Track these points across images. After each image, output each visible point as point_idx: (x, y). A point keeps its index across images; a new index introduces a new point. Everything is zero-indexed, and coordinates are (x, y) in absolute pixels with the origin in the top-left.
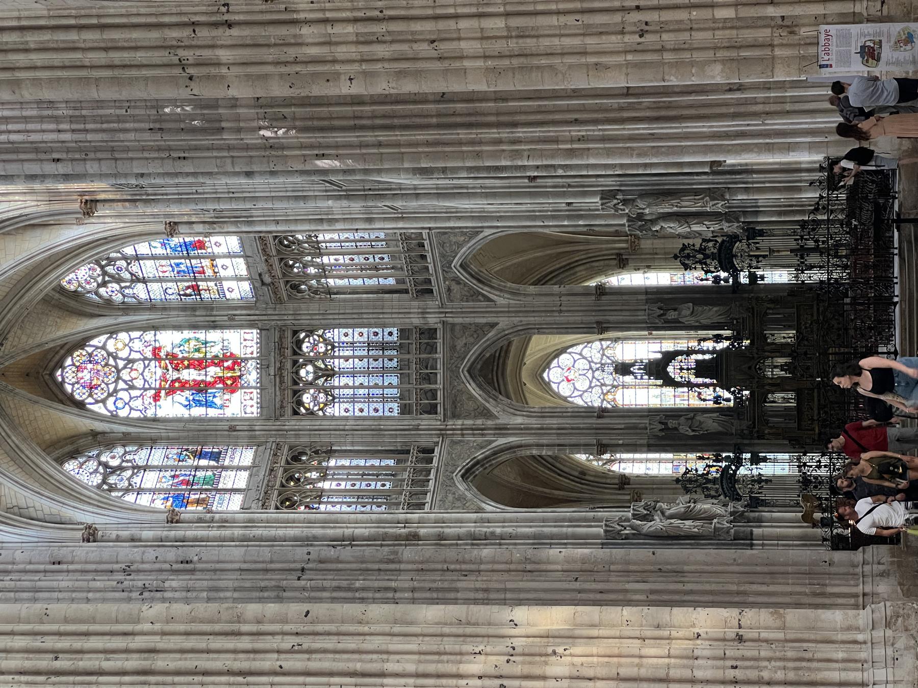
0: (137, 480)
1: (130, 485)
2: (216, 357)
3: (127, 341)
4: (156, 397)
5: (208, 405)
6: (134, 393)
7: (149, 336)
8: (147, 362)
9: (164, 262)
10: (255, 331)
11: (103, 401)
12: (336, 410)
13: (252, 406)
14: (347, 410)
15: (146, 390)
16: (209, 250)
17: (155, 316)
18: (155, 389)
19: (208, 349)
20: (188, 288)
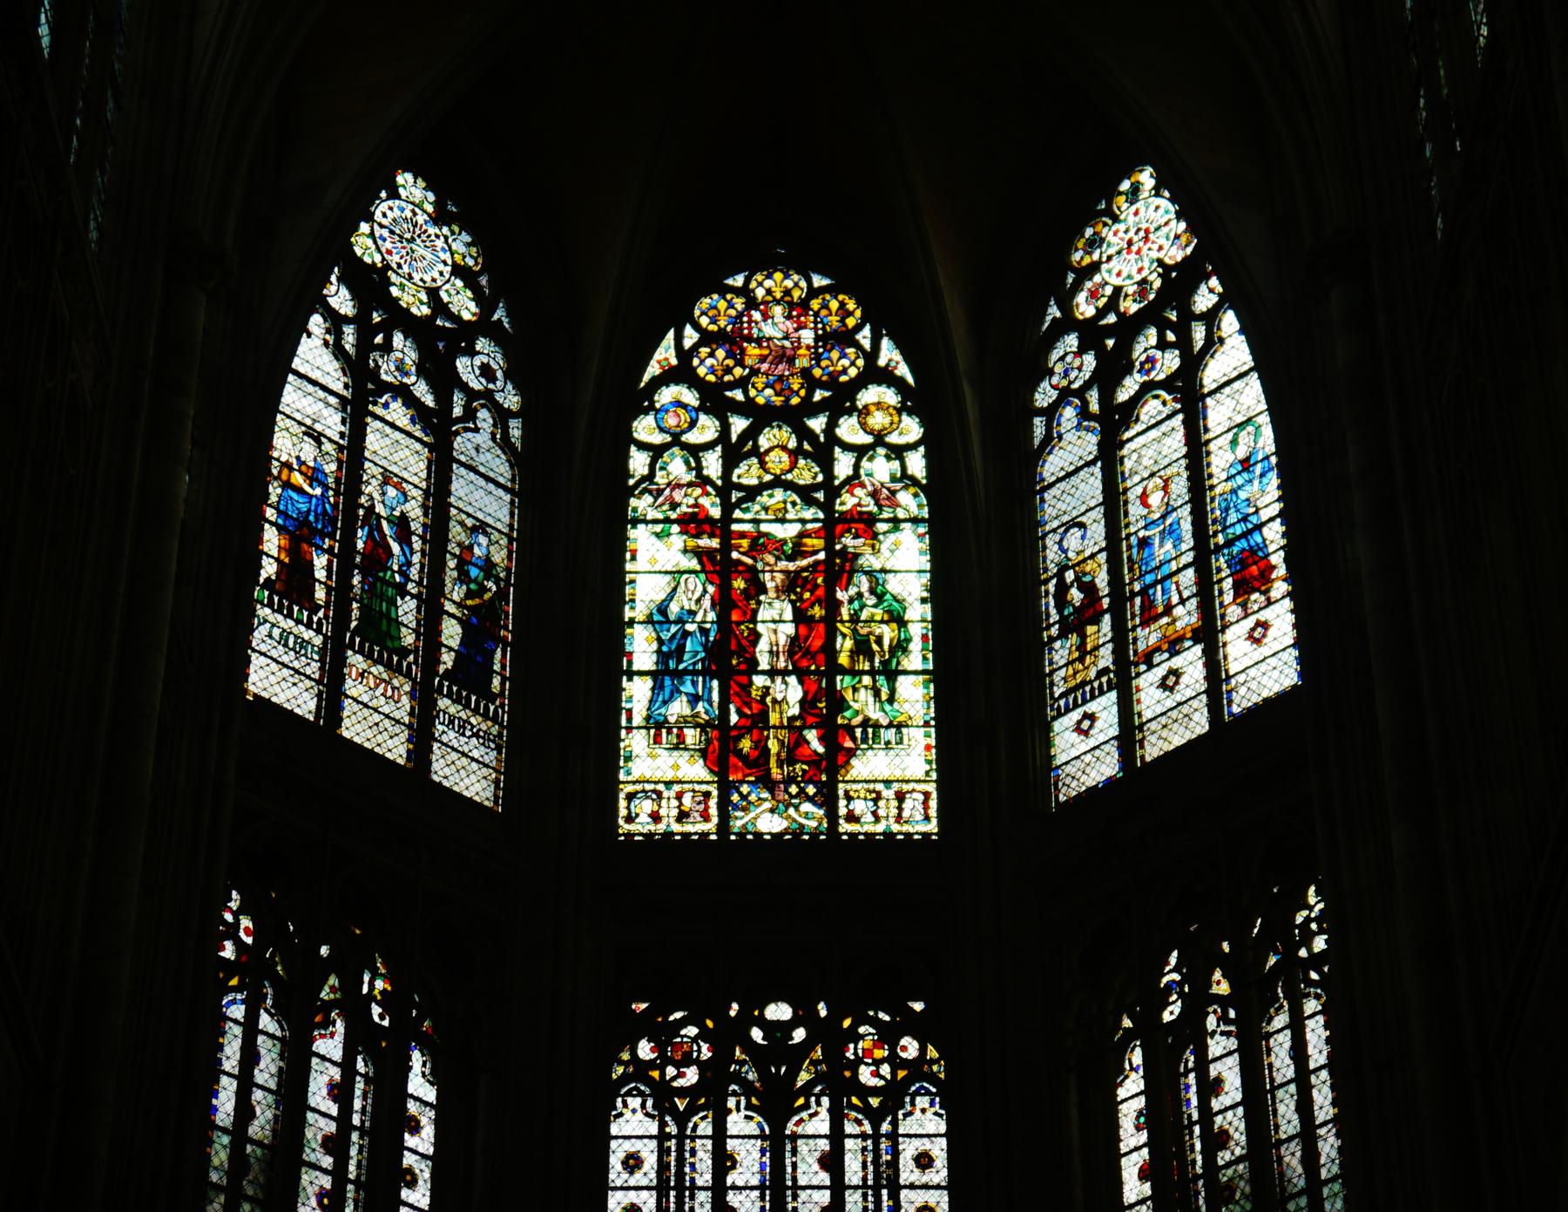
0: (398, 412)
1: (385, 387)
2: (838, 704)
3: (894, 439)
4: (694, 523)
5: (665, 675)
6: (713, 464)
7: (910, 503)
8: (820, 496)
9: (1180, 487)
10: (932, 827)
11: (682, 372)
12: (633, 1125)
13: (656, 817)
14: (632, 1163)
15: (724, 491)
16: (1234, 612)
17: (985, 515)
18: (727, 518)
19: (867, 680)
20: (1089, 589)
